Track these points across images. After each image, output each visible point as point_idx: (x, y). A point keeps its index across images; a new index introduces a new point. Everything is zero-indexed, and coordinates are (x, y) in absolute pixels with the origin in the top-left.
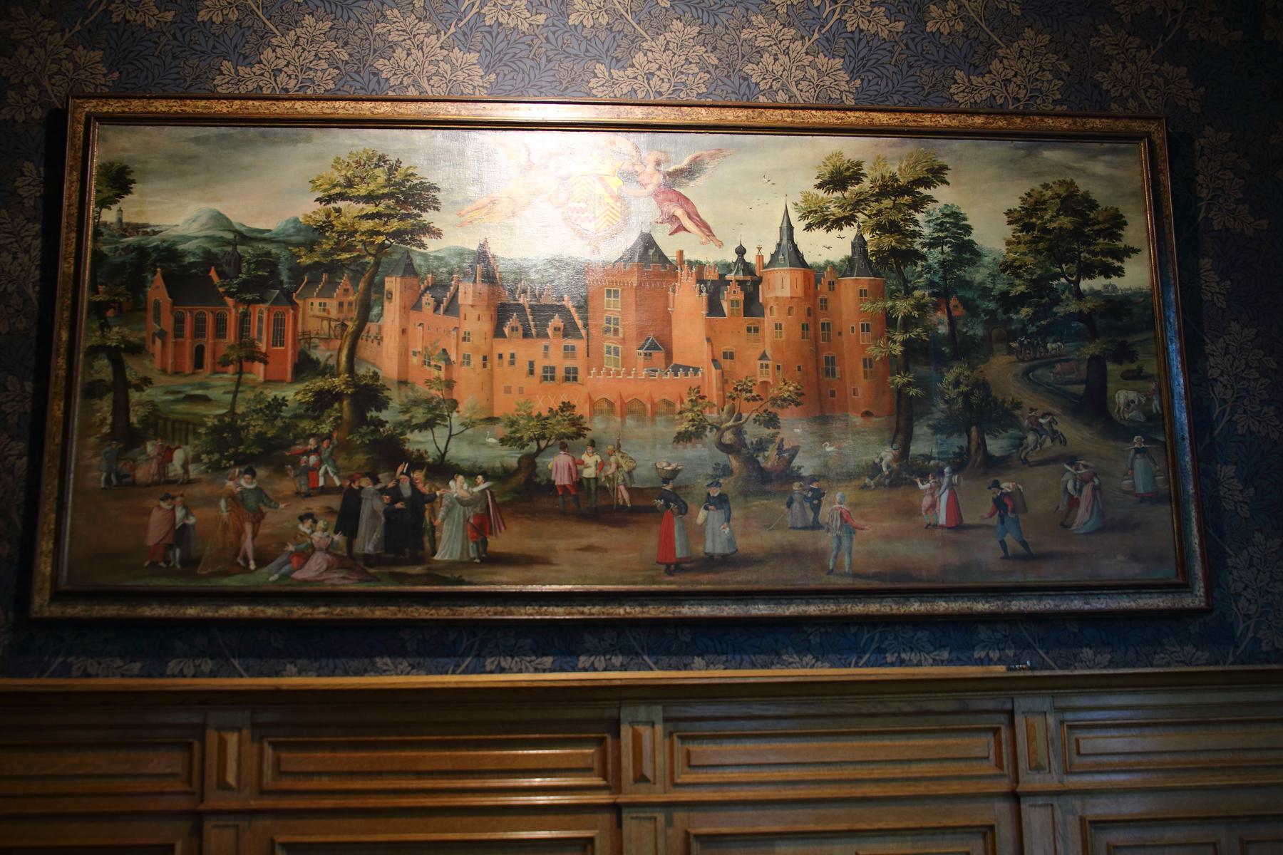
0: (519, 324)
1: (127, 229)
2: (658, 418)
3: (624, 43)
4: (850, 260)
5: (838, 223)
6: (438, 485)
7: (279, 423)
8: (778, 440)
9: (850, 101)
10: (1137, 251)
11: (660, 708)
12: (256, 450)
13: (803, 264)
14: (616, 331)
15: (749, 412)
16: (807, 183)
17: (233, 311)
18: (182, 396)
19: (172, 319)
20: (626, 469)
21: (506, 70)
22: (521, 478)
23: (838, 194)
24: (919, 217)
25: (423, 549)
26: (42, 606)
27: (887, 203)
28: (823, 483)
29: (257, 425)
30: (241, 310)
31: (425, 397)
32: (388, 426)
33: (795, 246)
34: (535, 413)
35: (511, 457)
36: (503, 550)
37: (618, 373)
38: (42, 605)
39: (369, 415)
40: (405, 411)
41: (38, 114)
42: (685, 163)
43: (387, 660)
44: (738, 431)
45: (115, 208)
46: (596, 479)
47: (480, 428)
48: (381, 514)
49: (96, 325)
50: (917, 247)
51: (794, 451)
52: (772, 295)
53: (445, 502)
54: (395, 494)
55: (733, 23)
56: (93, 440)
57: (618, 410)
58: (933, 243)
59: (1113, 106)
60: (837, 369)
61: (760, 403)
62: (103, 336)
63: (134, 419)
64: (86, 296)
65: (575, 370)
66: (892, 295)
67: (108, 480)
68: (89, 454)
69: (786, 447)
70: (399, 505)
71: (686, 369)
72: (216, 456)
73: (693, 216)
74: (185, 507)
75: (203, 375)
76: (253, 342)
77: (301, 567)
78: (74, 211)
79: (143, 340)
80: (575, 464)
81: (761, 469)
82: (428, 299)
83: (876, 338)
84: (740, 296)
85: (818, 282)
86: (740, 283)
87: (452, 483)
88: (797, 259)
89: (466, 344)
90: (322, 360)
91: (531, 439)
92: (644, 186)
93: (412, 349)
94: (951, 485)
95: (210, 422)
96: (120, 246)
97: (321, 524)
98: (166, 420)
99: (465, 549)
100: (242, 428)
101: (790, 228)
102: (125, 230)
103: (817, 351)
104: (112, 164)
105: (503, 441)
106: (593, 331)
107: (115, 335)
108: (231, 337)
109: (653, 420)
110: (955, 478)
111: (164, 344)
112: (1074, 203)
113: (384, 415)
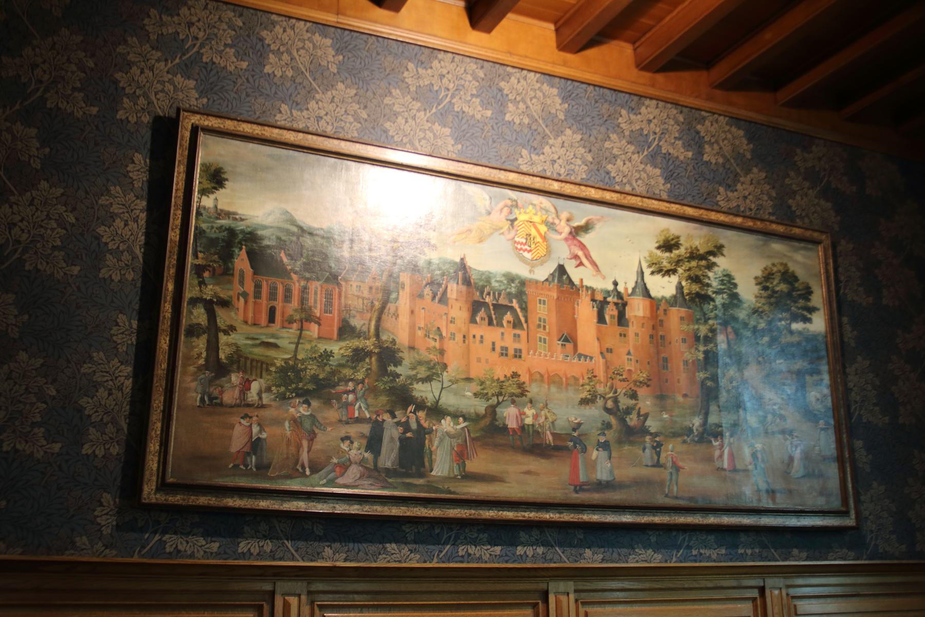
0: (485, 316)
1: (221, 214)
2: (569, 388)
3: (539, 138)
4: (675, 297)
5: (669, 272)
6: (434, 422)
7: (327, 369)
9: (664, 196)
10: (818, 309)
11: (572, 583)
12: (311, 387)
13: (649, 296)
14: (544, 327)
15: (622, 388)
16: (650, 245)
17: (297, 284)
18: (258, 342)
19: (253, 285)
20: (550, 420)
21: (468, 144)
22: (487, 421)
23: (667, 254)
24: (710, 274)
25: (423, 466)
26: (149, 493)
27: (694, 263)
29: (312, 369)
30: (303, 283)
31: (426, 359)
32: (401, 378)
33: (645, 284)
34: (496, 378)
35: (480, 406)
36: (475, 471)
37: (546, 356)
38: (149, 492)
39: (389, 369)
40: (413, 368)
41: (146, 119)
42: (582, 222)
43: (394, 545)
44: (616, 401)
45: (212, 197)
46: (533, 425)
47: (461, 384)
48: (397, 439)
49: (196, 282)
50: (710, 293)
51: (646, 416)
52: (633, 314)
53: (439, 434)
54: (406, 426)
55: (600, 137)
56: (192, 369)
57: (546, 380)
58: (717, 292)
59: (798, 220)
60: (669, 365)
61: (627, 383)
62: (201, 291)
63: (222, 356)
64: (190, 259)
65: (520, 351)
66: (698, 321)
67: (202, 400)
68: (188, 379)
70: (409, 435)
71: (586, 357)
72: (283, 389)
73: (588, 256)
74: (259, 424)
75: (275, 328)
76: (310, 308)
77: (342, 475)
78: (181, 194)
79: (231, 297)
80: (521, 414)
81: (628, 427)
82: (427, 291)
83: (690, 347)
84: (615, 313)
85: (658, 309)
86: (616, 304)
87: (443, 421)
88: (646, 293)
89: (452, 325)
90: (358, 327)
91: (493, 395)
92: (561, 233)
93: (418, 325)
94: (730, 444)
95: (279, 363)
96: (215, 225)
97: (356, 444)
98: (246, 358)
99: (451, 469)
100: (302, 370)
101: (642, 273)
102: (219, 214)
103: (658, 353)
104: (211, 165)
105: (476, 395)
106: (530, 325)
107: (209, 292)
108: (295, 303)
109: (567, 389)
110: (732, 440)
111: (246, 302)
112: (789, 277)
113: (399, 370)
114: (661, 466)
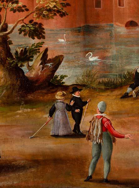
8: (42, 50)
28: (84, 93)
51: (57, 61)
61: (25, 13)
69: (49, 57)
114: (83, 136)
